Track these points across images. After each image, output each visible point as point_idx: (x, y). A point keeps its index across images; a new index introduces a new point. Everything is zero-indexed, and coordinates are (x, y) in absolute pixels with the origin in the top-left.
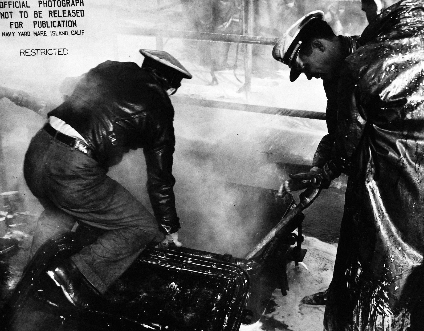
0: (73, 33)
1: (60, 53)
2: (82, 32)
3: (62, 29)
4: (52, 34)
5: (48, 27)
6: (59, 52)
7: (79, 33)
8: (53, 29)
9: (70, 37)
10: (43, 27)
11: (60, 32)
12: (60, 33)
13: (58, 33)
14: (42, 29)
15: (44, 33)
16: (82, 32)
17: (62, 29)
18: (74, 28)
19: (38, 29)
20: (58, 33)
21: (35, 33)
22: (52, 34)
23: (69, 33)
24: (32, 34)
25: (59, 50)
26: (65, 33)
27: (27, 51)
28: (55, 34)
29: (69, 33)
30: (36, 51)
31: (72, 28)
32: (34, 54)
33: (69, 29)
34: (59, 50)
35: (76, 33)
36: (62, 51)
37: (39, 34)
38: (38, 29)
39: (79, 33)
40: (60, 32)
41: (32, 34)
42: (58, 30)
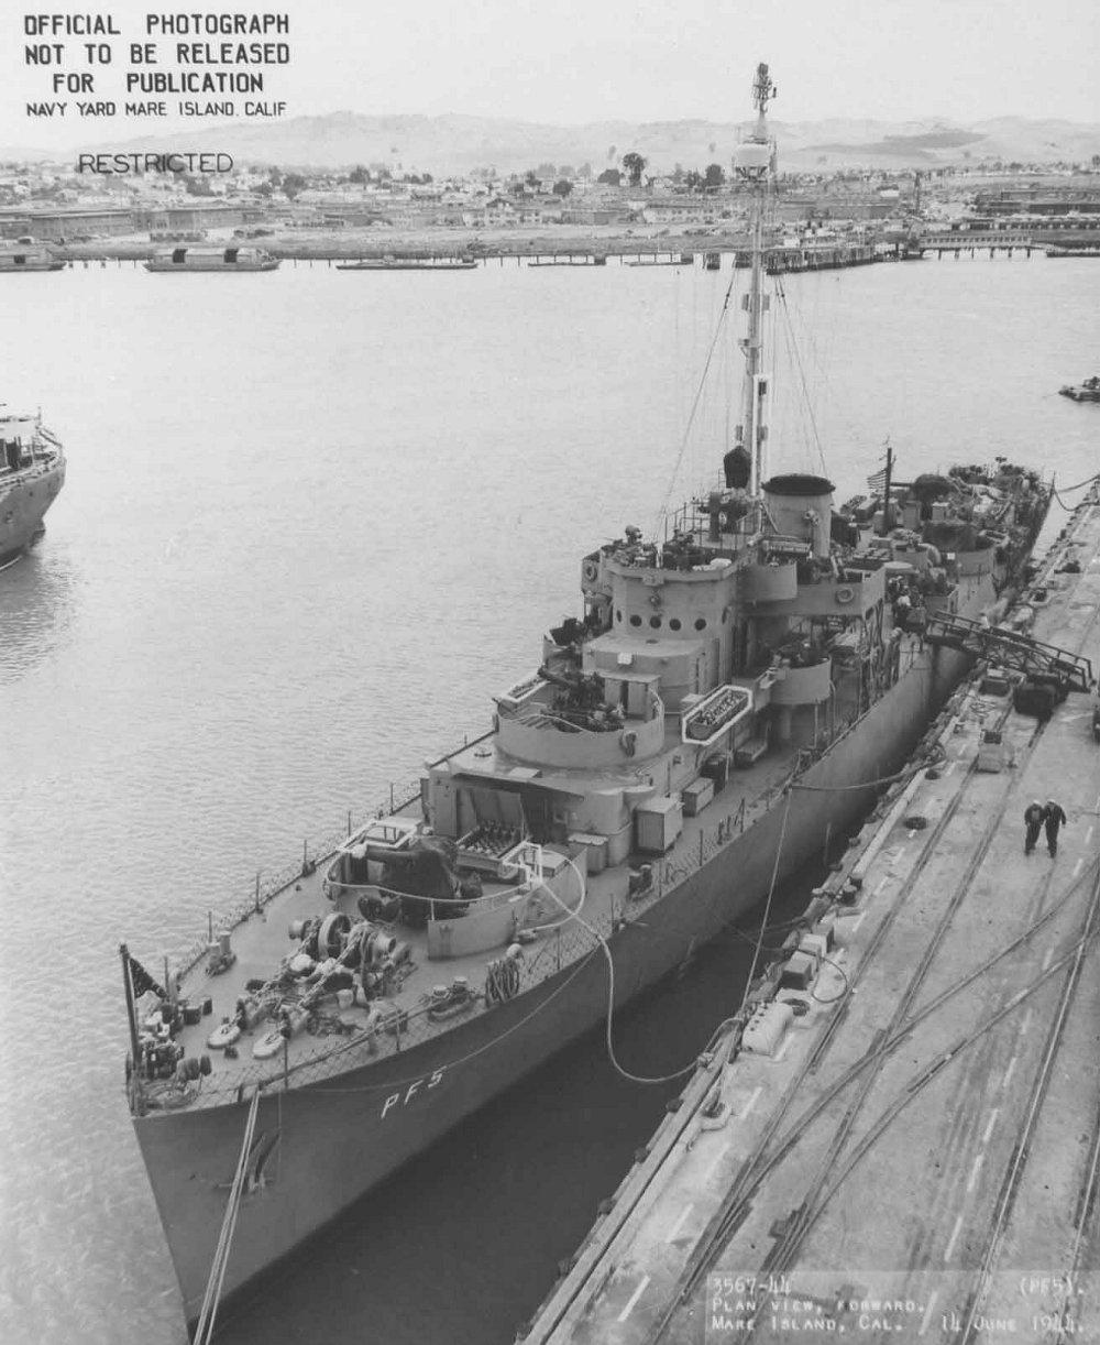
0: (251, 109)
1: (205, 167)
2: (280, 107)
5: (171, 90)
6: (202, 162)
8: (188, 96)
10: (157, 90)
11: (209, 105)
12: (210, 109)
13: (202, 109)
14: (154, 97)
15: (159, 108)
16: (280, 107)
18: (256, 96)
20: (202, 109)
21: (130, 108)
23: (239, 108)
24: (120, 109)
25: (204, 159)
26: (226, 109)
27: (102, 160)
28: (194, 111)
29: (239, 108)
30: (131, 162)
31: (248, 96)
32: (123, 167)
33: (239, 99)
34: (204, 159)
36: (213, 160)
38: (138, 96)
39: (270, 109)
40: (209, 105)
41: (120, 109)
42: (203, 99)
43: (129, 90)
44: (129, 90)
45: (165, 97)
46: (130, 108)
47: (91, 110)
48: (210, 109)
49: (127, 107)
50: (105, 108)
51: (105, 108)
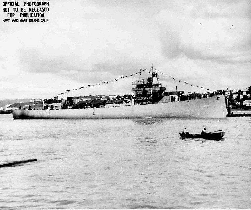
0: (42, 20)
2: (47, 20)
3: (36, 18)
4: (30, 21)
7: (45, 21)
8: (31, 18)
9: (40, 23)
10: (26, 17)
11: (35, 20)
12: (35, 21)
13: (33, 21)
14: (25, 18)
15: (26, 20)
18: (43, 18)
19: (23, 18)
20: (33, 21)
21: (21, 20)
24: (19, 20)
26: (37, 20)
31: (42, 18)
33: (40, 18)
35: (44, 21)
37: (23, 21)
38: (23, 18)
39: (45, 21)
41: (19, 20)
42: (34, 19)
43: (21, 17)
44: (21, 17)
46: (21, 20)
48: (35, 21)
50: (17, 20)
51: (17, 20)
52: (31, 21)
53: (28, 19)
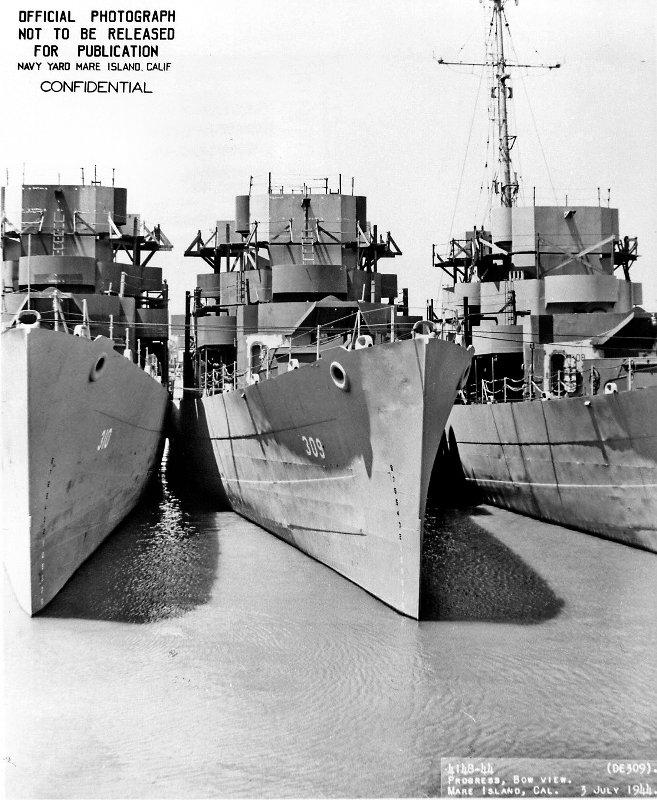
2: (167, 66)
3: (130, 60)
4: (111, 67)
5: (104, 55)
7: (162, 67)
8: (114, 59)
10: (96, 55)
14: (93, 59)
15: (95, 66)
16: (167, 66)
17: (130, 60)
18: (154, 60)
19: (84, 59)
22: (111, 67)
23: (143, 66)
24: (73, 66)
26: (136, 67)
28: (117, 68)
31: (149, 59)
33: (143, 61)
35: (155, 67)
38: (84, 59)
39: (162, 67)
41: (73, 66)
42: (122, 61)
45: (100, 59)
47: (56, 67)
49: (77, 65)
52: (115, 67)
53: (103, 62)
